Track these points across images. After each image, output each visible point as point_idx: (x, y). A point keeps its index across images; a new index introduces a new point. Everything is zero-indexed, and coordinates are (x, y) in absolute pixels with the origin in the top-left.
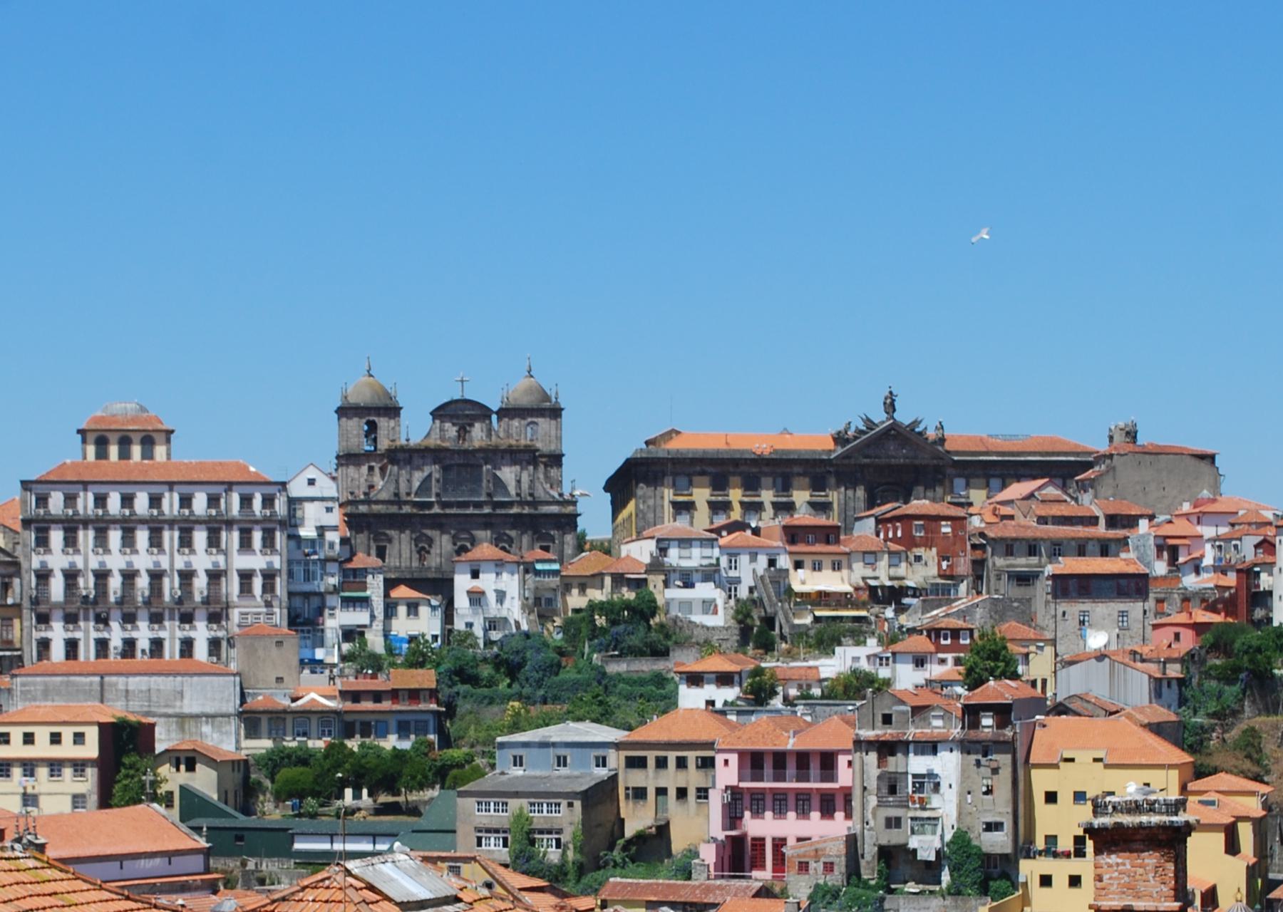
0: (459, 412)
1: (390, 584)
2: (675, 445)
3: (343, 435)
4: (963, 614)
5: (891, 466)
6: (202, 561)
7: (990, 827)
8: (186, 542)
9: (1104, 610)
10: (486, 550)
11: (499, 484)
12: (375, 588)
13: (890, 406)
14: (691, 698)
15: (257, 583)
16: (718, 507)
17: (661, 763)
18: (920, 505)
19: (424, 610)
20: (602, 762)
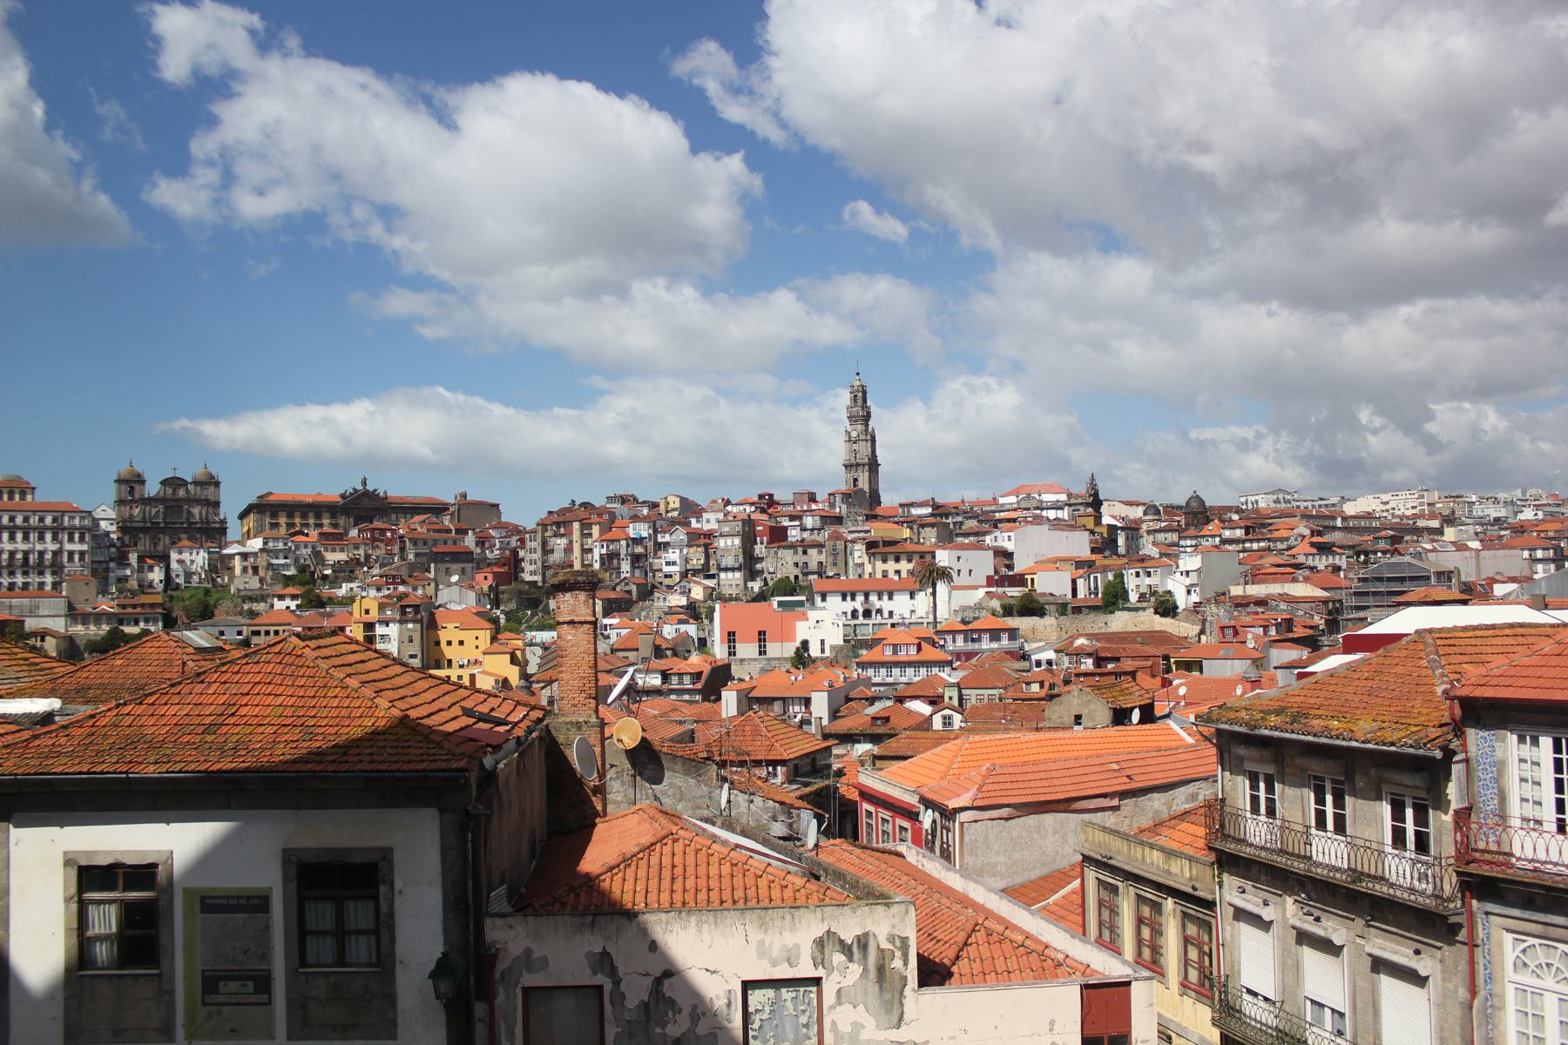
0: (172, 482)
1: (141, 559)
2: (271, 498)
3: (119, 491)
4: (398, 568)
5: (364, 508)
6: (51, 546)
7: (412, 656)
8: (41, 538)
9: (454, 566)
10: (186, 543)
11: (190, 514)
12: (133, 558)
13: (364, 483)
14: (279, 605)
15: (77, 557)
16: (290, 525)
17: (267, 633)
18: (377, 524)
19: (156, 569)
20: (240, 633)
